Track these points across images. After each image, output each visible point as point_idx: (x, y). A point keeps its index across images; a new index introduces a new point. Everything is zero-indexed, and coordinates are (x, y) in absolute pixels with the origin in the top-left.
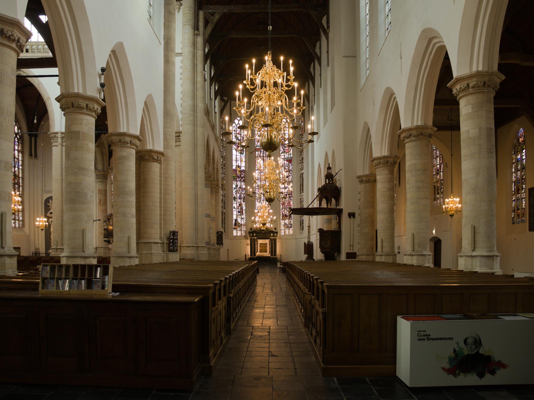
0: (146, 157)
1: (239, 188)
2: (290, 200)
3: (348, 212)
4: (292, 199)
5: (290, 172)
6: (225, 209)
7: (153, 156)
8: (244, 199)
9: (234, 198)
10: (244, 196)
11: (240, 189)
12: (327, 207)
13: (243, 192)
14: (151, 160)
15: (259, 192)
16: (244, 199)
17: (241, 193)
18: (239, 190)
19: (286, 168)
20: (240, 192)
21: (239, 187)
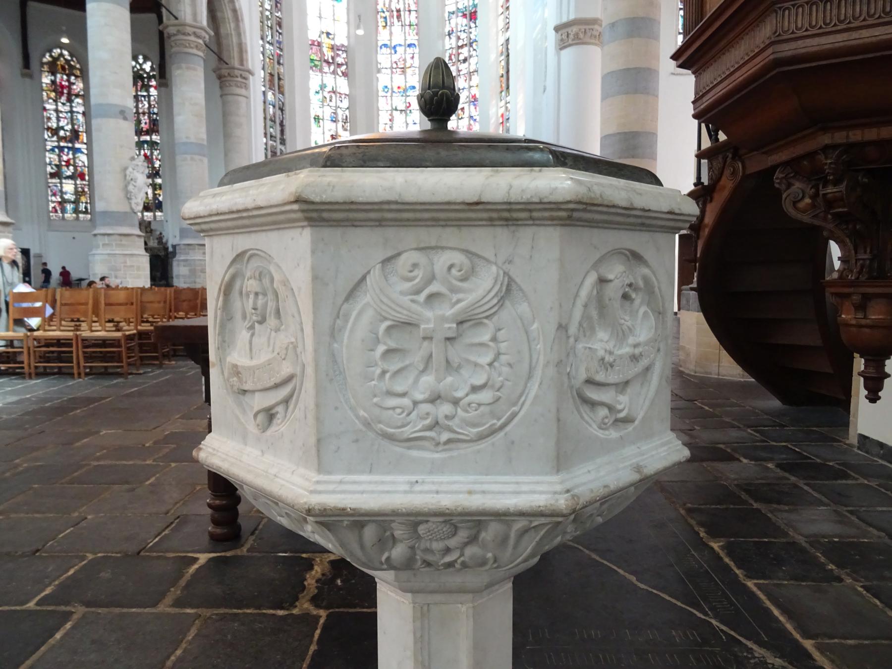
1: (329, 92)
2: (472, 122)
4: (477, 120)
6: (283, 142)
8: (345, 123)
9: (315, 118)
10: (346, 117)
11: (333, 95)
13: (341, 105)
15: (387, 104)
16: (345, 121)
17: (337, 107)
18: (331, 97)
19: (461, 38)
20: (333, 104)
21: (329, 89)
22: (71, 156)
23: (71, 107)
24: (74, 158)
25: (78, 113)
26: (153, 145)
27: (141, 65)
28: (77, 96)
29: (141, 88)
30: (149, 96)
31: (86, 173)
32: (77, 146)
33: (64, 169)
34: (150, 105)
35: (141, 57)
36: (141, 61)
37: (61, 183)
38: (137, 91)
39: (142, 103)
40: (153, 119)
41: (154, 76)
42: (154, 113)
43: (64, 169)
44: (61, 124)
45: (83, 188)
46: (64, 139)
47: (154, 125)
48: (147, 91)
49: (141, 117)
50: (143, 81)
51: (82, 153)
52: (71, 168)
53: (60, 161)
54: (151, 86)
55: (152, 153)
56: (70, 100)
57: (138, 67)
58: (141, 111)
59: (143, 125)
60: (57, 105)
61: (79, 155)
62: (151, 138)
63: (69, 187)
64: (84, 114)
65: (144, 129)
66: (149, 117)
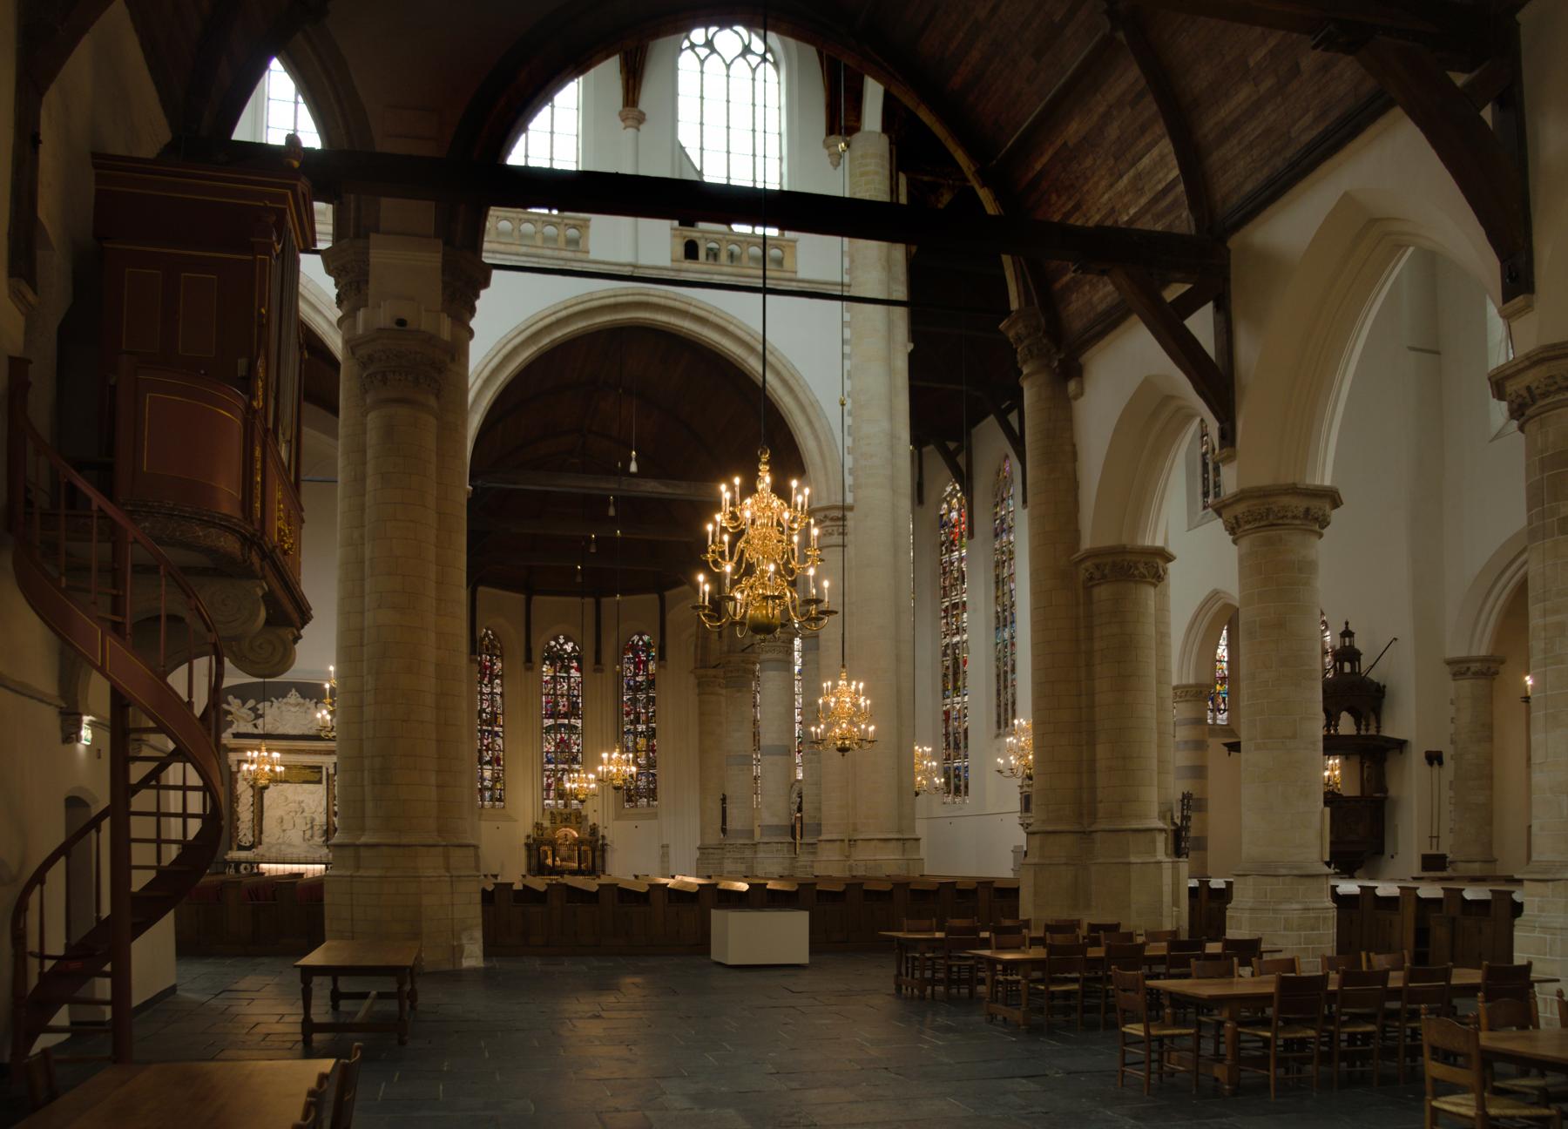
0: (1137, 568)
3: (1424, 751)
5: (957, 628)
7: (1158, 567)
12: (1359, 733)
14: (1150, 580)
22: (490, 740)
23: (492, 688)
24: (493, 742)
25: (497, 694)
26: (572, 729)
27: (561, 645)
28: (497, 676)
29: (561, 669)
30: (569, 678)
31: (502, 757)
32: (496, 729)
33: (485, 753)
34: (569, 687)
35: (562, 637)
36: (562, 641)
37: (482, 769)
38: (555, 672)
39: (561, 684)
40: (573, 702)
41: (575, 658)
42: (574, 696)
43: (485, 753)
44: (484, 706)
45: (498, 774)
46: (484, 722)
47: (573, 708)
48: (568, 672)
49: (559, 699)
50: (563, 662)
51: (499, 736)
52: (490, 752)
53: (482, 744)
54: (573, 667)
55: (570, 738)
56: (491, 681)
57: (558, 647)
58: (559, 692)
59: (561, 708)
60: (481, 687)
61: (497, 738)
62: (569, 722)
63: (487, 774)
64: (502, 695)
65: (562, 712)
66: (567, 699)
